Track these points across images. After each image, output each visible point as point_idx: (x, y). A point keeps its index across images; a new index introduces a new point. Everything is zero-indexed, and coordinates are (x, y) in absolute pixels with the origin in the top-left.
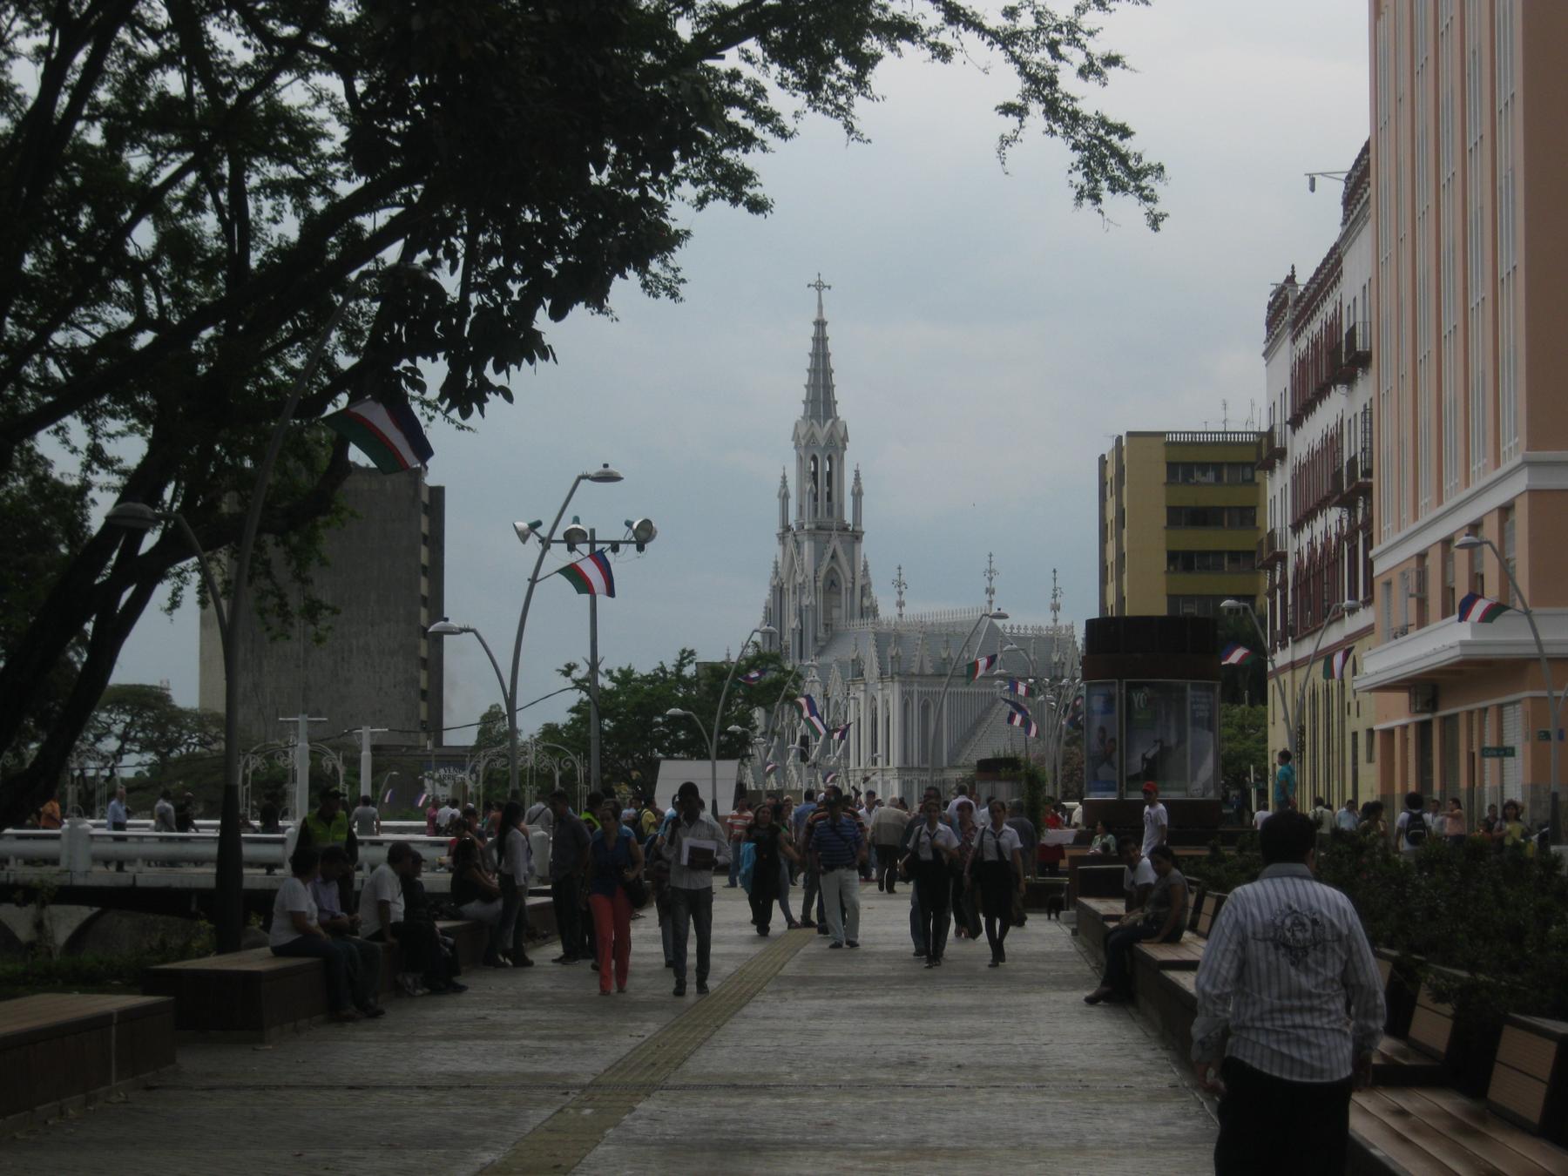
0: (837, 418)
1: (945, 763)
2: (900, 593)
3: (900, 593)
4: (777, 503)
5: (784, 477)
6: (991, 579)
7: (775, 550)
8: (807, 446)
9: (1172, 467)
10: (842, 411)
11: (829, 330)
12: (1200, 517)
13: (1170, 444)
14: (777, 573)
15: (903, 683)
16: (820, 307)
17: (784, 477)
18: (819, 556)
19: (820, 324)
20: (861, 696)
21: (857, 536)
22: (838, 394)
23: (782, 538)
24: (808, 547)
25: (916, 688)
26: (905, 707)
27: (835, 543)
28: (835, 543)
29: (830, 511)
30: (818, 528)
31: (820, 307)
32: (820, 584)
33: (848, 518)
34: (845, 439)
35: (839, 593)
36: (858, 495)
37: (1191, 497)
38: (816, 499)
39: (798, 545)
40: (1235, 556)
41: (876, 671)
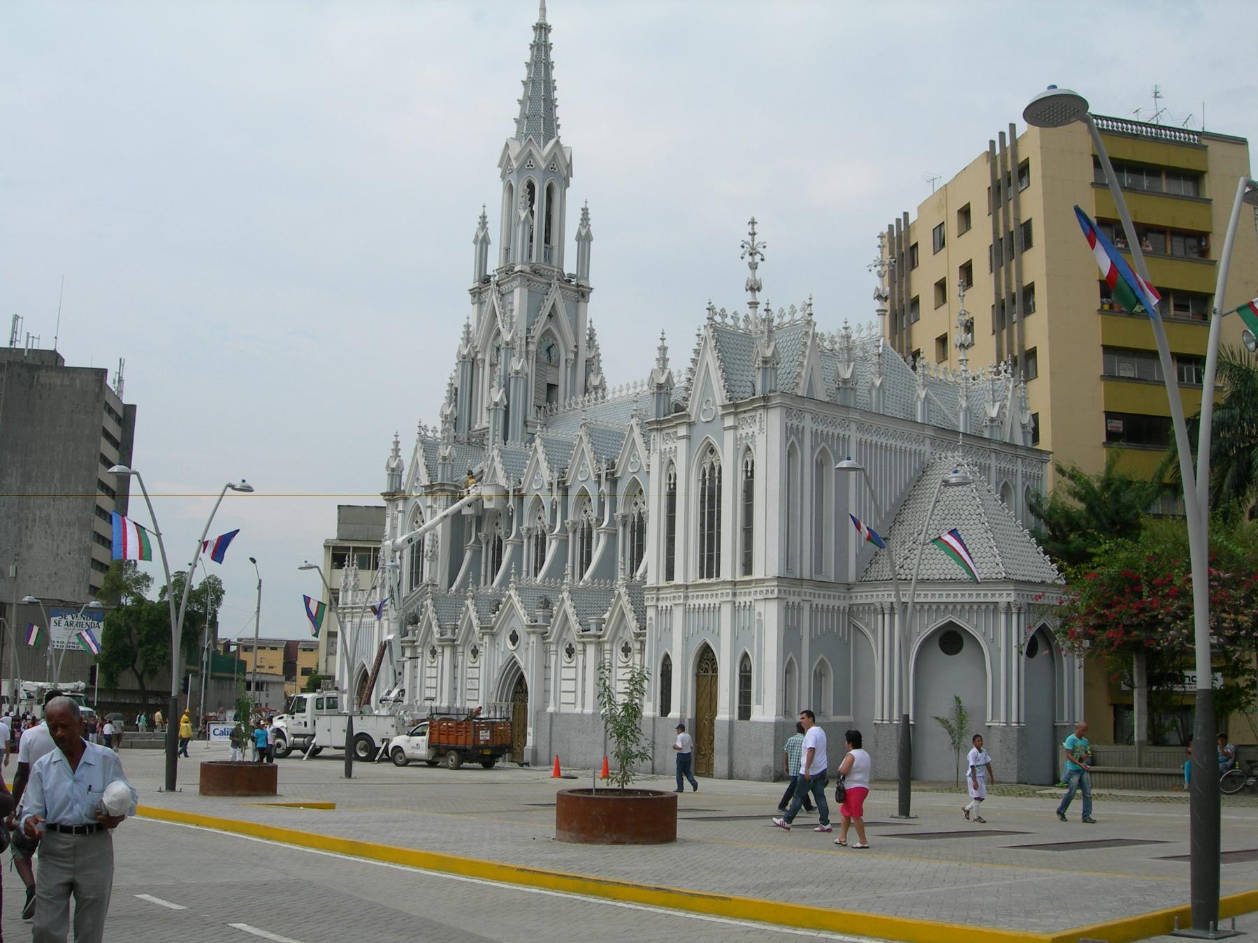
1: (852, 578)
2: (753, 266)
3: (753, 266)
4: (471, 252)
7: (467, 311)
8: (520, 170)
10: (566, 135)
11: (551, 38)
14: (468, 339)
15: (788, 411)
19: (542, 29)
20: (682, 446)
21: (582, 293)
22: (562, 113)
23: (477, 294)
24: (518, 298)
25: (808, 423)
26: (790, 454)
27: (555, 295)
28: (555, 295)
29: (548, 256)
30: (535, 272)
31: (543, 9)
32: (532, 348)
33: (570, 267)
36: (584, 240)
37: (1129, 208)
41: (719, 396)
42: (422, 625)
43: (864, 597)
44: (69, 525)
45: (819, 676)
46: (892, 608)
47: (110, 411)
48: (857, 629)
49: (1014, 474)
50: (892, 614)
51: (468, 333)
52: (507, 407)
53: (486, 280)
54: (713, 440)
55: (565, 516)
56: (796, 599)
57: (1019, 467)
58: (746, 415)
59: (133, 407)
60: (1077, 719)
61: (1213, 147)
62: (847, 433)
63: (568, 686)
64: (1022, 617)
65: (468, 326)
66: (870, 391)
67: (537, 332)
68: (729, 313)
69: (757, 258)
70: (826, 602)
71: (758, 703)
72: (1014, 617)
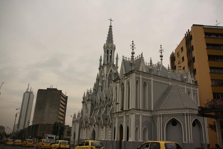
2: (133, 49)
3: (133, 49)
4: (99, 62)
5: (101, 56)
6: (161, 53)
9: (206, 34)
13: (204, 28)
14: (98, 76)
16: (111, 24)
17: (101, 56)
18: (107, 71)
19: (111, 26)
23: (99, 69)
25: (141, 76)
27: (111, 68)
28: (111, 68)
31: (111, 24)
33: (115, 63)
39: (103, 68)
42: (83, 124)
43: (155, 113)
44: (55, 113)
45: (144, 132)
46: (160, 116)
47: (63, 97)
48: (153, 121)
49: (191, 90)
50: (160, 117)
51: (98, 75)
52: (102, 86)
53: (101, 66)
54: (123, 82)
55: (107, 103)
56: (138, 114)
57: (192, 88)
58: (129, 76)
59: (67, 97)
60: (207, 142)
62: (151, 79)
63: (102, 134)
64: (190, 116)
65: (98, 74)
66: (157, 72)
67: (108, 74)
68: (128, 58)
69: (134, 48)
70: (144, 114)
71: (130, 137)
72: (188, 116)
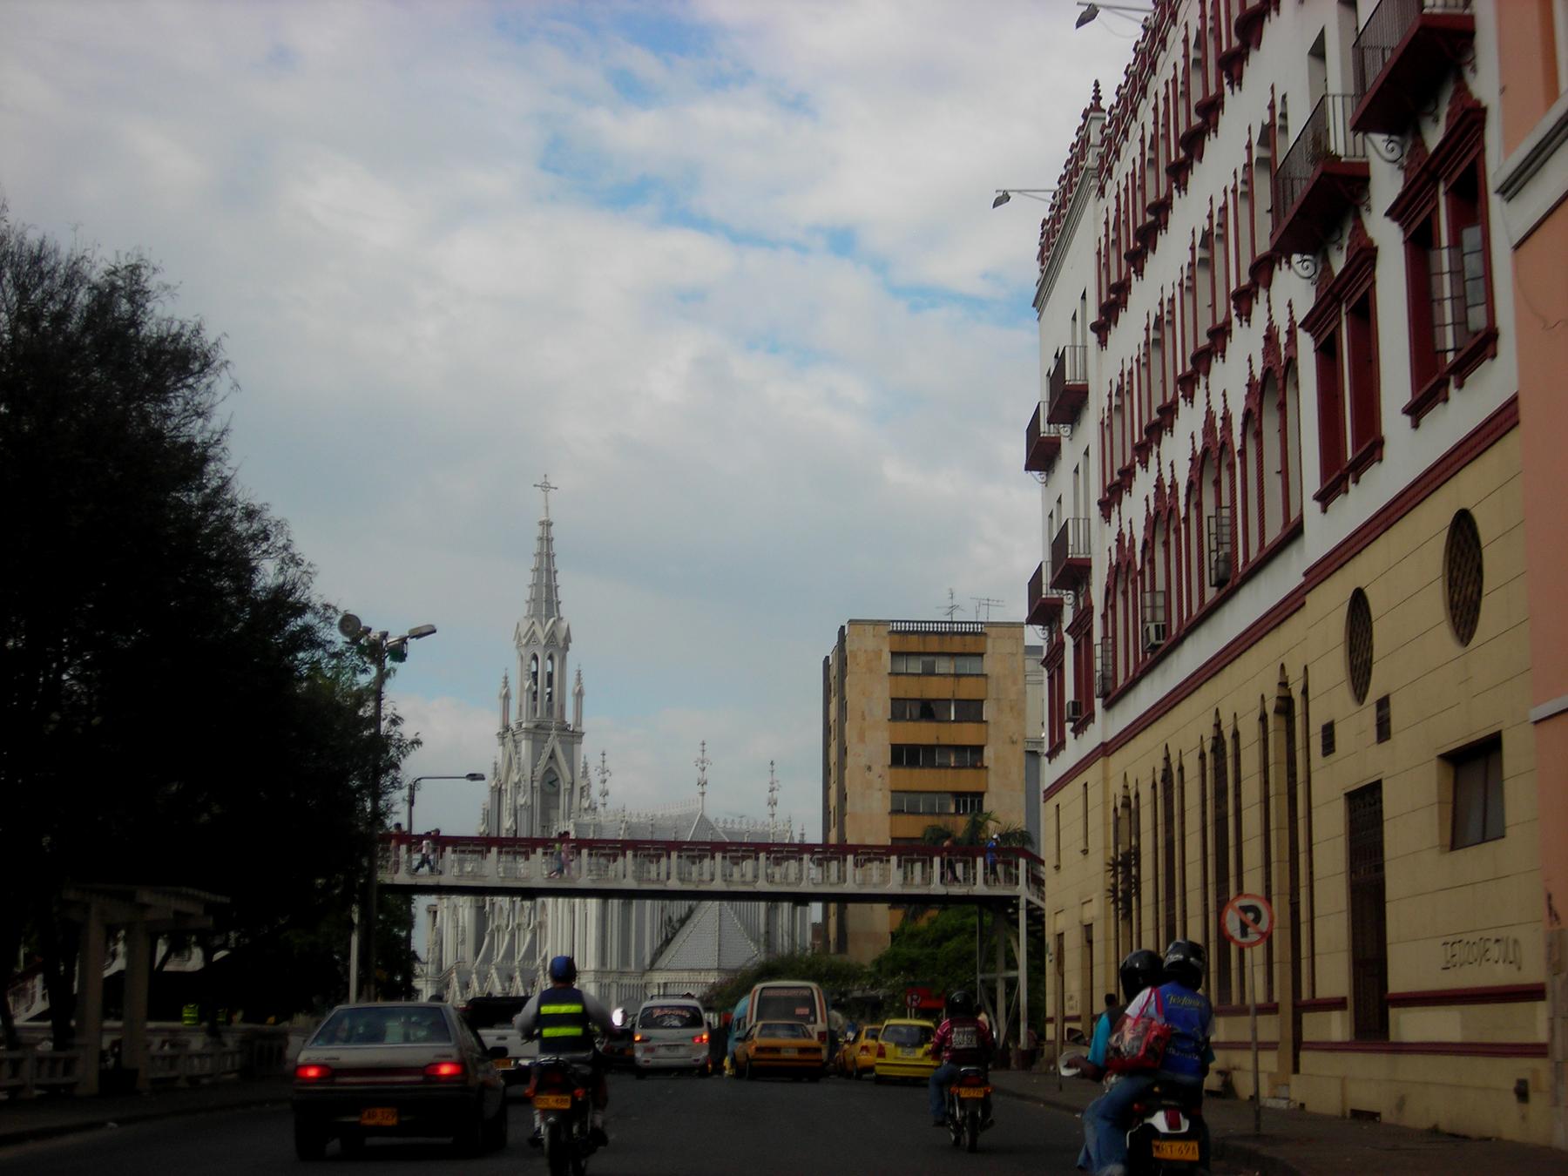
0: (560, 619)
12: (928, 710)
23: (502, 736)
24: (525, 746)
27: (553, 742)
28: (553, 742)
29: (550, 709)
33: (570, 718)
34: (567, 639)
35: (557, 794)
36: (579, 695)
38: (535, 699)
39: (516, 744)
40: (960, 749)
42: (451, 991)
53: (507, 728)
56: (607, 981)
61: (992, 632)
67: (540, 771)
